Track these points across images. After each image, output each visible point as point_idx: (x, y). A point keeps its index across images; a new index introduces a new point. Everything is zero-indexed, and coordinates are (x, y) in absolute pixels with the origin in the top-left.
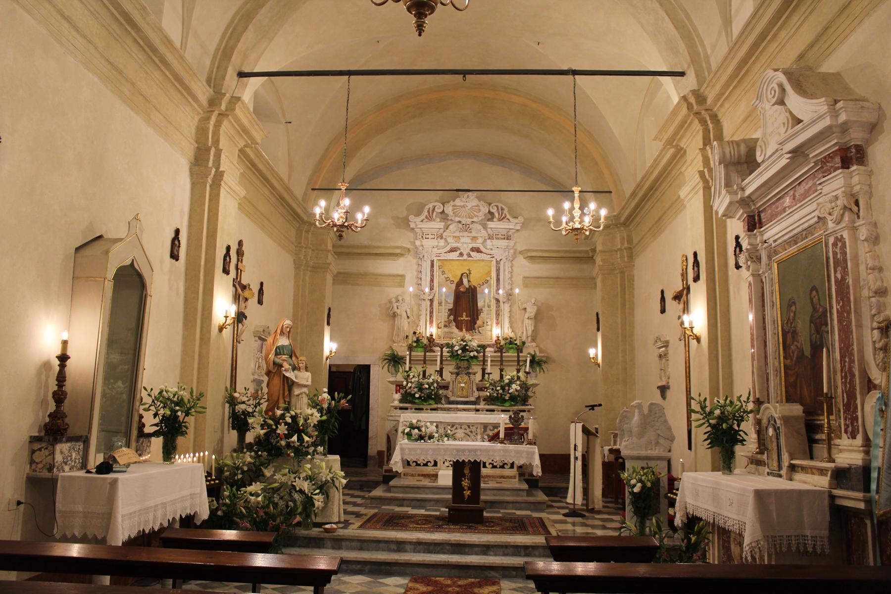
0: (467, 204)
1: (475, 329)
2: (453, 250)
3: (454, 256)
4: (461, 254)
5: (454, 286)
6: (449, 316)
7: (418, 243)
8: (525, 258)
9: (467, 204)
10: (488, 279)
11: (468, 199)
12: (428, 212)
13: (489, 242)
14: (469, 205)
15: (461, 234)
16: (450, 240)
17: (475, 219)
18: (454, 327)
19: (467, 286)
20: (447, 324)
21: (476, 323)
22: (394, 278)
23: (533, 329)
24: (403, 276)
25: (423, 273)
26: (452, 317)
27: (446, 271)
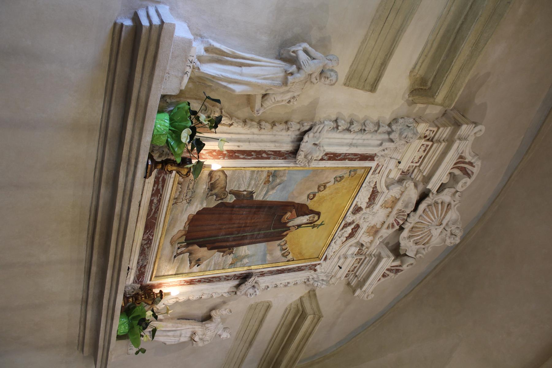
0: (440, 229)
1: (188, 245)
2: (374, 195)
3: (363, 199)
4: (358, 210)
5: (302, 199)
6: (236, 194)
7: (422, 128)
8: (301, 298)
9: (440, 229)
10: (290, 257)
11: (449, 233)
12: (471, 164)
13: (355, 250)
14: (436, 232)
15: (395, 212)
16: (395, 191)
17: (405, 234)
18: (205, 206)
19: (289, 224)
20: (216, 191)
21: (201, 246)
22: (378, 62)
23: (167, 343)
24: (373, 88)
25: (359, 136)
26: (231, 199)
27: (338, 185)
